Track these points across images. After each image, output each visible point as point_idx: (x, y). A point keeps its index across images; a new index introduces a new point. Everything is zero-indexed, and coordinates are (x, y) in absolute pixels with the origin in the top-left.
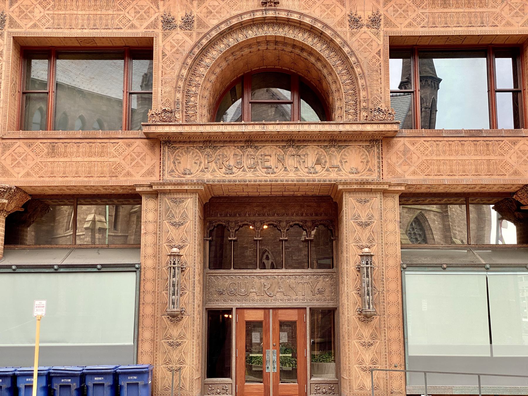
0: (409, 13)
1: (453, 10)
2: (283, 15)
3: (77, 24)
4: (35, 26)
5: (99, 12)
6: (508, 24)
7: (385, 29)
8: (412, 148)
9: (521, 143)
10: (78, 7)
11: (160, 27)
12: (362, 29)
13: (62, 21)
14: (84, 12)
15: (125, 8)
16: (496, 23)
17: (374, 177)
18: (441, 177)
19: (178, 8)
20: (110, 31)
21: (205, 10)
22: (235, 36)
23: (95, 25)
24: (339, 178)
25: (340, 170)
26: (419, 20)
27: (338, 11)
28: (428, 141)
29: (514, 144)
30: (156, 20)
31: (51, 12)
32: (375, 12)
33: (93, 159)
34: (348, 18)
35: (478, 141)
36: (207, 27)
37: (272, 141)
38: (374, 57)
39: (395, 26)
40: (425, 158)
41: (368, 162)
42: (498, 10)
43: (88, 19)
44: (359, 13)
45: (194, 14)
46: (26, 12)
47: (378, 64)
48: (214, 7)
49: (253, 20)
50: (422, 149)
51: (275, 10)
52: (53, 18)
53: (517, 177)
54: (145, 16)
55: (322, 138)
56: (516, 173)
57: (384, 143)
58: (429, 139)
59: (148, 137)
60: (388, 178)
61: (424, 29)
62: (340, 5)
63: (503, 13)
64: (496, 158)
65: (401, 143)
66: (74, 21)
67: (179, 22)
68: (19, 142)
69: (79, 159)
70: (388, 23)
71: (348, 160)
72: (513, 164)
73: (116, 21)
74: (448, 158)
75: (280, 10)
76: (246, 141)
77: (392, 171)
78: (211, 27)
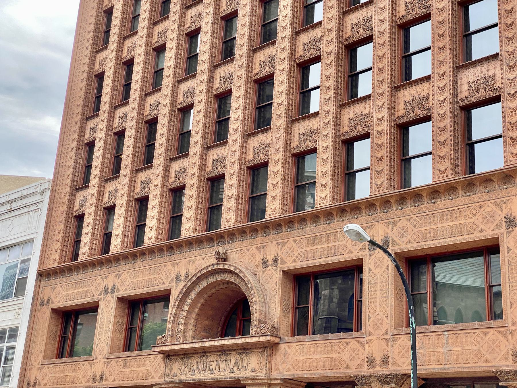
6: (350, 252)
7: (281, 266)
8: (288, 351)
9: (352, 343)
11: (175, 282)
12: (269, 268)
16: (343, 252)
17: (263, 374)
18: (303, 372)
20: (154, 288)
22: (202, 283)
24: (245, 375)
25: (246, 370)
26: (299, 256)
28: (298, 345)
29: (348, 344)
31: (132, 280)
32: (276, 254)
33: (140, 369)
34: (262, 261)
35: (326, 343)
37: (215, 351)
38: (273, 287)
39: (285, 263)
40: (295, 358)
41: (261, 363)
42: (344, 243)
44: (268, 257)
47: (275, 291)
50: (294, 351)
53: (348, 370)
55: (238, 348)
56: (347, 367)
57: (274, 349)
58: (299, 343)
59: (162, 352)
60: (274, 375)
61: (302, 263)
62: (258, 253)
63: (347, 244)
64: (337, 355)
65: (283, 348)
68: (113, 360)
69: (135, 369)
70: (283, 262)
71: (250, 362)
72: (346, 360)
74: (308, 357)
76: (203, 352)
77: (277, 369)
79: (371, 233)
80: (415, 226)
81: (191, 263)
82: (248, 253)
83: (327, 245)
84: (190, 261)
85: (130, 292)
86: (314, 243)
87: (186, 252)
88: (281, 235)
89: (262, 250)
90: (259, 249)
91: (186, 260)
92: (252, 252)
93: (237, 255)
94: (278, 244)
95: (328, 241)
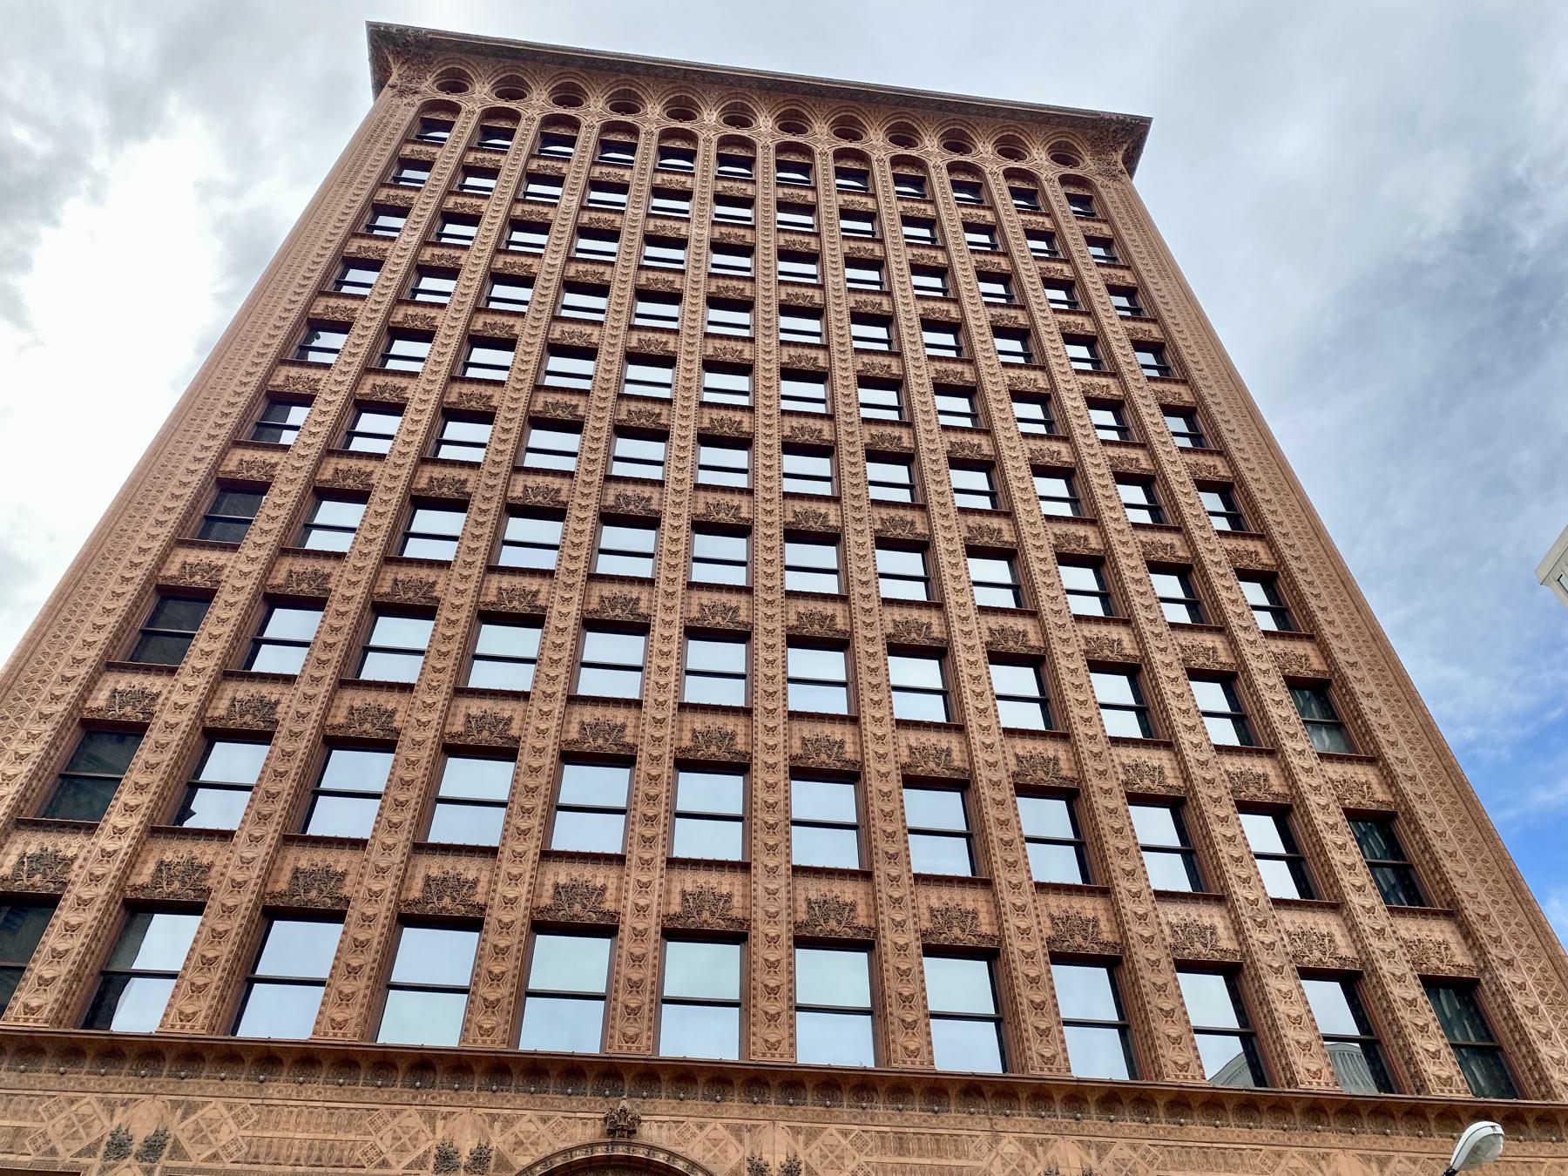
0: (846, 1162)
1: (915, 1160)
2: (641, 1154)
3: (289, 1157)
4: (215, 1156)
5: (331, 1137)
10: (297, 1124)
11: (431, 1167)
13: (263, 1150)
14: (305, 1135)
15: (377, 1130)
19: (468, 1132)
21: (512, 1139)
23: (319, 1159)
27: (731, 1151)
30: (426, 1154)
31: (249, 1133)
32: (791, 1156)
34: (747, 1165)
36: (512, 1169)
42: (984, 1164)
43: (310, 1148)
44: (767, 1157)
45: (493, 1145)
46: (207, 1131)
48: (528, 1134)
49: (589, 1160)
51: (629, 1144)
52: (250, 1146)
54: (410, 1146)
66: (284, 1152)
67: (464, 1159)
73: (358, 1154)
75: (637, 1145)
78: (518, 1169)
79: (1049, 1155)
80: (1151, 1164)
81: (497, 1125)
82: (701, 1135)
83: (937, 1162)
84: (494, 1118)
85: (229, 1166)
86: (902, 1149)
87: (479, 1089)
88: (800, 1109)
89: (746, 1136)
90: (736, 1131)
91: (480, 1111)
92: (713, 1135)
93: (664, 1133)
94: (796, 1131)
95: (939, 1152)
